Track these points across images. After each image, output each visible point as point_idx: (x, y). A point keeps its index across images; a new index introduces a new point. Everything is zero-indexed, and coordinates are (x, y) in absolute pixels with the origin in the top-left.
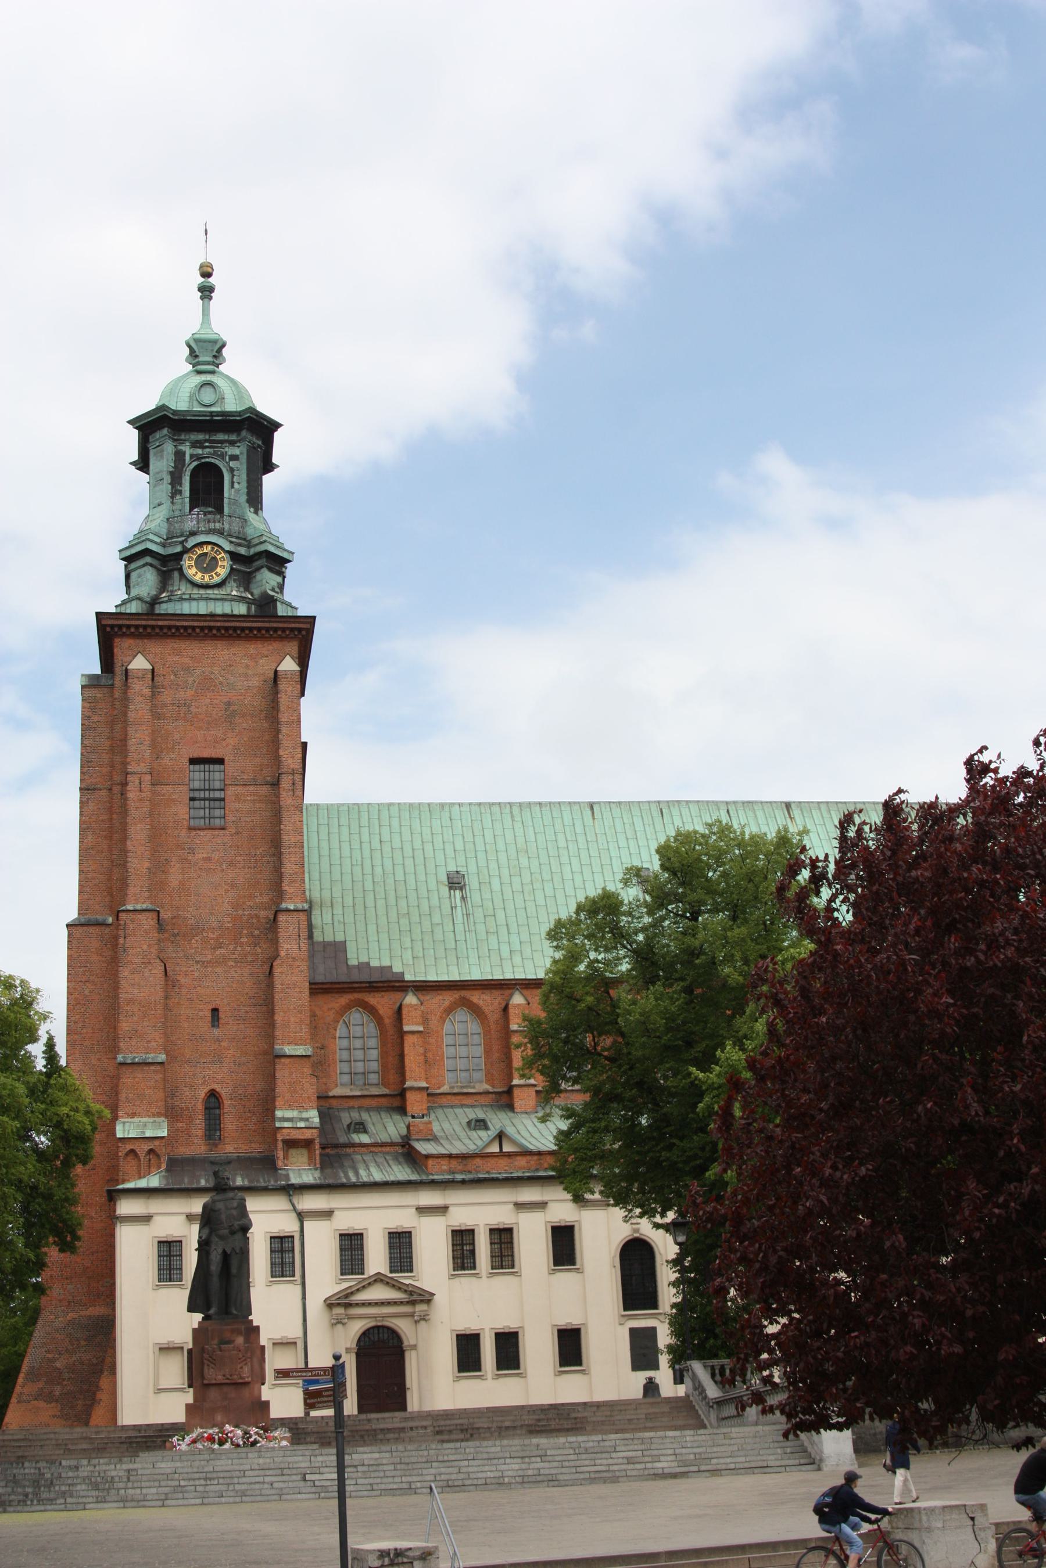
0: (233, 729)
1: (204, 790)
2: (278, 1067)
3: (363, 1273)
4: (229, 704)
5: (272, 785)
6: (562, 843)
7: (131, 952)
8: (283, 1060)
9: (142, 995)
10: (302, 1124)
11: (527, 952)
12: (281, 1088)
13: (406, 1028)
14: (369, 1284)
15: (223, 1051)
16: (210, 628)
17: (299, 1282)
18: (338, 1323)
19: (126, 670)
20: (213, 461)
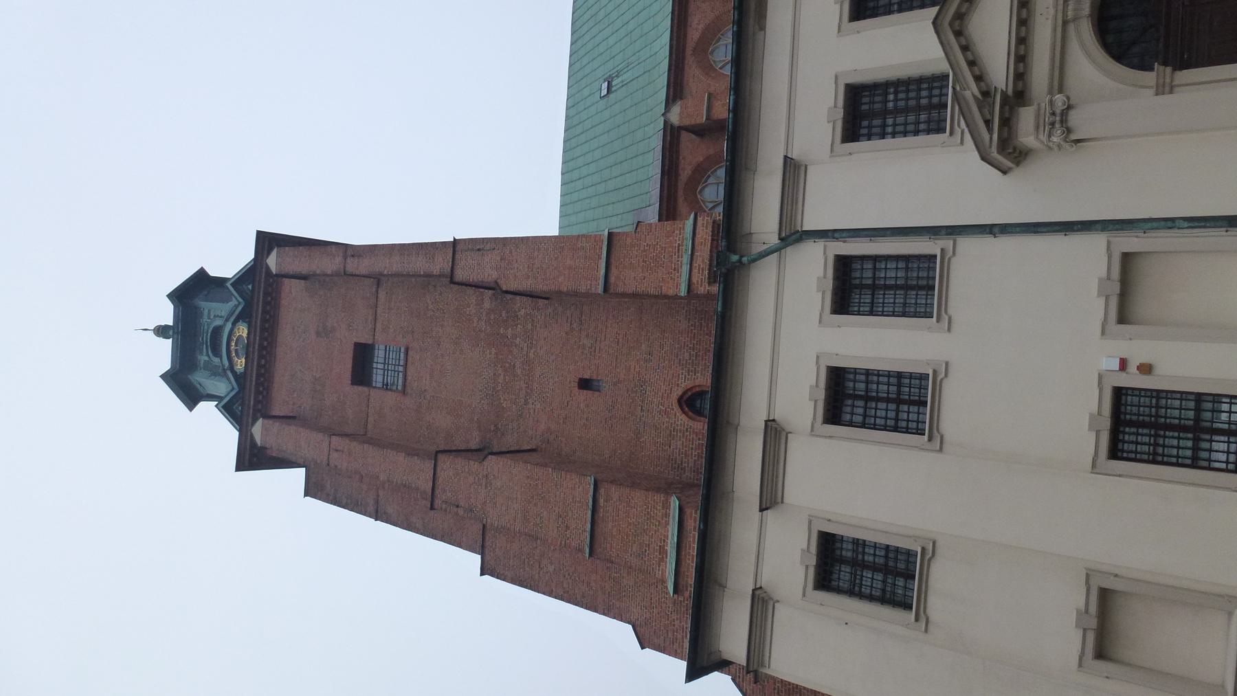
2: (620, 290)
3: (946, 77)
4: (318, 334)
5: (378, 285)
8: (612, 279)
9: (519, 496)
12: (649, 286)
14: (965, 49)
15: (631, 376)
16: (262, 348)
17: (947, 243)
18: (1063, 121)
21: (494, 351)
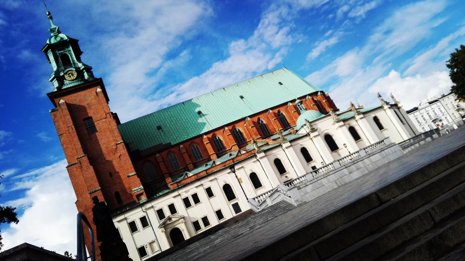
0: (91, 109)
1: (89, 125)
6: (179, 112)
7: (83, 167)
8: (130, 177)
10: (139, 190)
11: (180, 136)
13: (158, 162)
19: (59, 104)
20: (64, 53)
21: (107, 153)
